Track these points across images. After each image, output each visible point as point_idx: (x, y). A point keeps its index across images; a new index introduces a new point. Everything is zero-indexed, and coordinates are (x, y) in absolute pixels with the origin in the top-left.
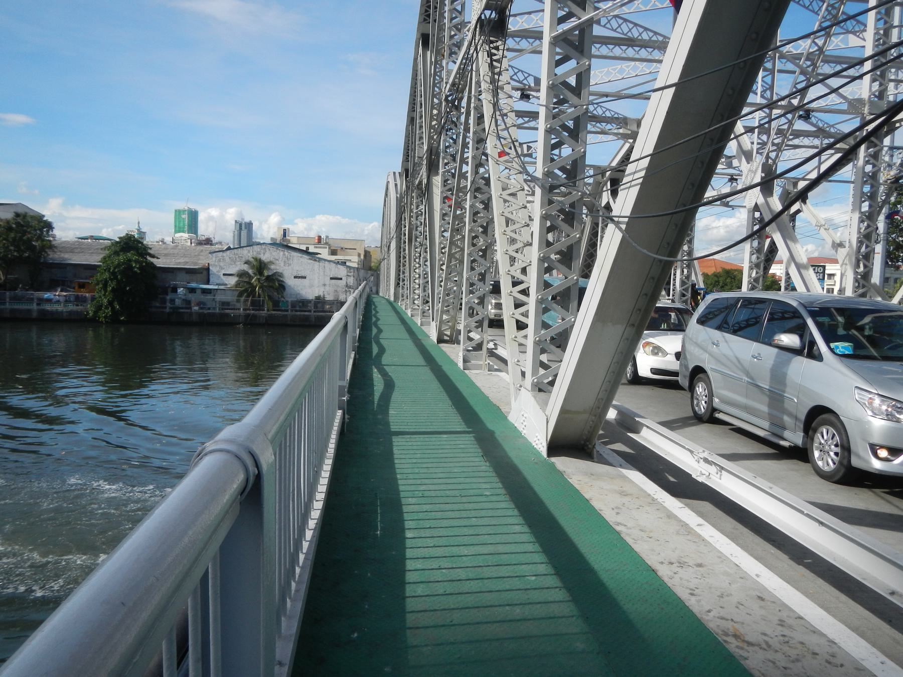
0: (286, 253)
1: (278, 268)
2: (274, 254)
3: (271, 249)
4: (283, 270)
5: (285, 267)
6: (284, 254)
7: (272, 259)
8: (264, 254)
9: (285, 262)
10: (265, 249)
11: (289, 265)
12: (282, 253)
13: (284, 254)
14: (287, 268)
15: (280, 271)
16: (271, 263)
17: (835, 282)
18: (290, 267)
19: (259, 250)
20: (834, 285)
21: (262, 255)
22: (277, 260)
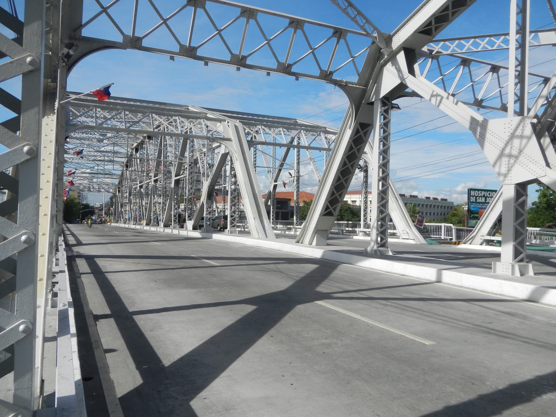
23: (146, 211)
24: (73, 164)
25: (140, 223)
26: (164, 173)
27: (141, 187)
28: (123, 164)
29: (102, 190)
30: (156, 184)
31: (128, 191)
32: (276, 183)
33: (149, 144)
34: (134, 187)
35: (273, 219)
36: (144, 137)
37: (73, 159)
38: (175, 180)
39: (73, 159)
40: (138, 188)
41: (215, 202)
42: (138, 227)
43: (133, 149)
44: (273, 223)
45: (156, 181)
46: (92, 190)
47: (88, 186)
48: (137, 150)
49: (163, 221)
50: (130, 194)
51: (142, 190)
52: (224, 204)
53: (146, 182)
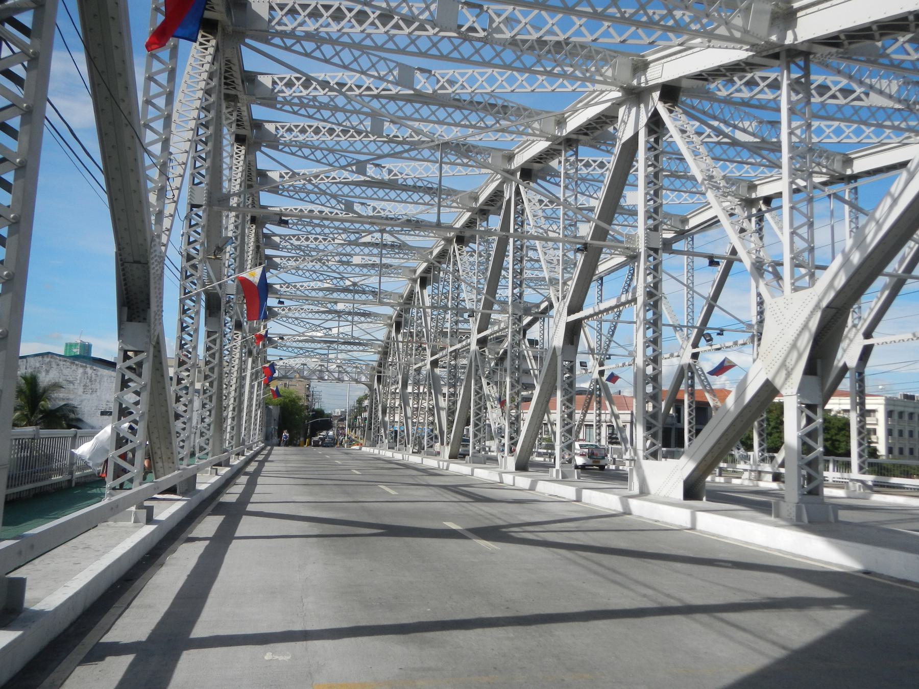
0: (89, 371)
1: (71, 396)
2: (66, 372)
3: (61, 363)
4: (82, 401)
5: (84, 396)
6: (85, 373)
7: (61, 380)
8: (47, 372)
9: (85, 386)
10: (50, 362)
11: (94, 391)
12: (81, 370)
13: (85, 373)
14: (88, 396)
15: (75, 403)
16: (57, 386)
17: (877, 420)
18: (94, 395)
19: (38, 365)
20: (876, 424)
21: (44, 374)
22: (71, 382)
23: (450, 423)
24: (290, 320)
25: (430, 450)
26: (514, 314)
27: (435, 364)
28: (389, 321)
29: (346, 378)
30: (484, 351)
31: (400, 377)
32: (868, 342)
33: (460, 255)
34: (415, 367)
35: (860, 456)
36: (449, 241)
37: (290, 309)
38: (568, 324)
39: (290, 309)
40: (428, 366)
41: (607, 403)
42: (431, 463)
43: (415, 281)
44: (861, 468)
45: (482, 342)
46: (326, 378)
47: (319, 368)
48: (424, 282)
49: (511, 451)
50: (405, 385)
51: (438, 371)
52: (598, 412)
53: (451, 349)
